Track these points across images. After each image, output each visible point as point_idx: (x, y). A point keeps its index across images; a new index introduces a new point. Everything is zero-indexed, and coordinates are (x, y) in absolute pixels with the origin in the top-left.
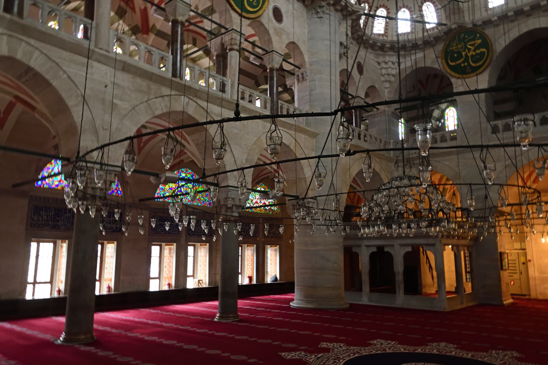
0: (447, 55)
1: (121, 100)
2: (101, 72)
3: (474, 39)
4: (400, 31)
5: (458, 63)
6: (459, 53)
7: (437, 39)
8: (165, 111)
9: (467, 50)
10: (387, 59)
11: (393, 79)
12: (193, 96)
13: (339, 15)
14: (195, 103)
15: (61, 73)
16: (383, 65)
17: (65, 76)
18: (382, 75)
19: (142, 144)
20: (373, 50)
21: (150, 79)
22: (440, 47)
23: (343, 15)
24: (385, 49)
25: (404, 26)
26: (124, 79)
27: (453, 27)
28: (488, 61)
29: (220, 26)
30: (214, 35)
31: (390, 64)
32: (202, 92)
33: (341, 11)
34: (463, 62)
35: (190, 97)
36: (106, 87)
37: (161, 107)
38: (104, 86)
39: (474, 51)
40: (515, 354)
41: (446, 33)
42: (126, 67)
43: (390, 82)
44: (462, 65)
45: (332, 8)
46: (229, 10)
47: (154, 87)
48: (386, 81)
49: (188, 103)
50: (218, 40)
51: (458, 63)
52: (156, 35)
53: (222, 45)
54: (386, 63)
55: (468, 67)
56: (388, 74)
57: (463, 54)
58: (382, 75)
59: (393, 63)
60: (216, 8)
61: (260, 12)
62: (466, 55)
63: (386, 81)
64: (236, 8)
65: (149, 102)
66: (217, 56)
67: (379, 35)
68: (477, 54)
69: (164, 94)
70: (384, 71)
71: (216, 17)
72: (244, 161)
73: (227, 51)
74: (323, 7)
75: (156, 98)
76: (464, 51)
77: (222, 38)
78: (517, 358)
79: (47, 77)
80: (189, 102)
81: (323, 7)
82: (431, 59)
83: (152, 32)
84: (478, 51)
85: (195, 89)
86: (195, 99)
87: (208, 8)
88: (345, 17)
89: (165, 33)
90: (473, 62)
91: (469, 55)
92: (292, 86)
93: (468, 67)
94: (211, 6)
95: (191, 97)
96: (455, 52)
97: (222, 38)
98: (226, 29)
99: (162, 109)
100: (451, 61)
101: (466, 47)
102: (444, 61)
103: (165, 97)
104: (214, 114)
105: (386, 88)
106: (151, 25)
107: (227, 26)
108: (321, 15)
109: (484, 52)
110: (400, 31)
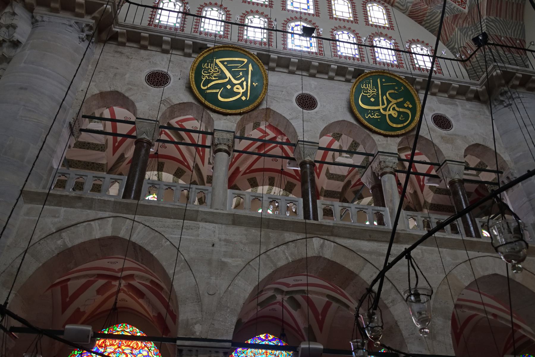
1: (232, 257)
2: (208, 231)
8: (290, 260)
12: (329, 235)
14: (332, 244)
15: (164, 240)
17: (168, 243)
19: (320, 317)
21: (268, 227)
26: (237, 233)
29: (368, 155)
32: (339, 227)
35: (324, 237)
36: (213, 245)
37: (283, 256)
38: (211, 245)
42: (236, 220)
45: (521, 90)
46: (369, 136)
47: (274, 235)
49: (322, 246)
50: (369, 170)
52: (325, 196)
53: (374, 173)
60: (358, 141)
64: (377, 130)
65: (268, 253)
66: (372, 188)
69: (287, 240)
71: (360, 149)
74: (506, 92)
75: (278, 246)
77: (372, 167)
79: (148, 248)
80: (324, 243)
81: (506, 92)
83: (321, 195)
85: (329, 226)
86: (332, 238)
87: (352, 144)
89: (333, 191)
94: (353, 141)
95: (326, 237)
97: (372, 167)
99: (287, 258)
103: (290, 243)
104: (365, 252)
106: (319, 189)
107: (373, 153)
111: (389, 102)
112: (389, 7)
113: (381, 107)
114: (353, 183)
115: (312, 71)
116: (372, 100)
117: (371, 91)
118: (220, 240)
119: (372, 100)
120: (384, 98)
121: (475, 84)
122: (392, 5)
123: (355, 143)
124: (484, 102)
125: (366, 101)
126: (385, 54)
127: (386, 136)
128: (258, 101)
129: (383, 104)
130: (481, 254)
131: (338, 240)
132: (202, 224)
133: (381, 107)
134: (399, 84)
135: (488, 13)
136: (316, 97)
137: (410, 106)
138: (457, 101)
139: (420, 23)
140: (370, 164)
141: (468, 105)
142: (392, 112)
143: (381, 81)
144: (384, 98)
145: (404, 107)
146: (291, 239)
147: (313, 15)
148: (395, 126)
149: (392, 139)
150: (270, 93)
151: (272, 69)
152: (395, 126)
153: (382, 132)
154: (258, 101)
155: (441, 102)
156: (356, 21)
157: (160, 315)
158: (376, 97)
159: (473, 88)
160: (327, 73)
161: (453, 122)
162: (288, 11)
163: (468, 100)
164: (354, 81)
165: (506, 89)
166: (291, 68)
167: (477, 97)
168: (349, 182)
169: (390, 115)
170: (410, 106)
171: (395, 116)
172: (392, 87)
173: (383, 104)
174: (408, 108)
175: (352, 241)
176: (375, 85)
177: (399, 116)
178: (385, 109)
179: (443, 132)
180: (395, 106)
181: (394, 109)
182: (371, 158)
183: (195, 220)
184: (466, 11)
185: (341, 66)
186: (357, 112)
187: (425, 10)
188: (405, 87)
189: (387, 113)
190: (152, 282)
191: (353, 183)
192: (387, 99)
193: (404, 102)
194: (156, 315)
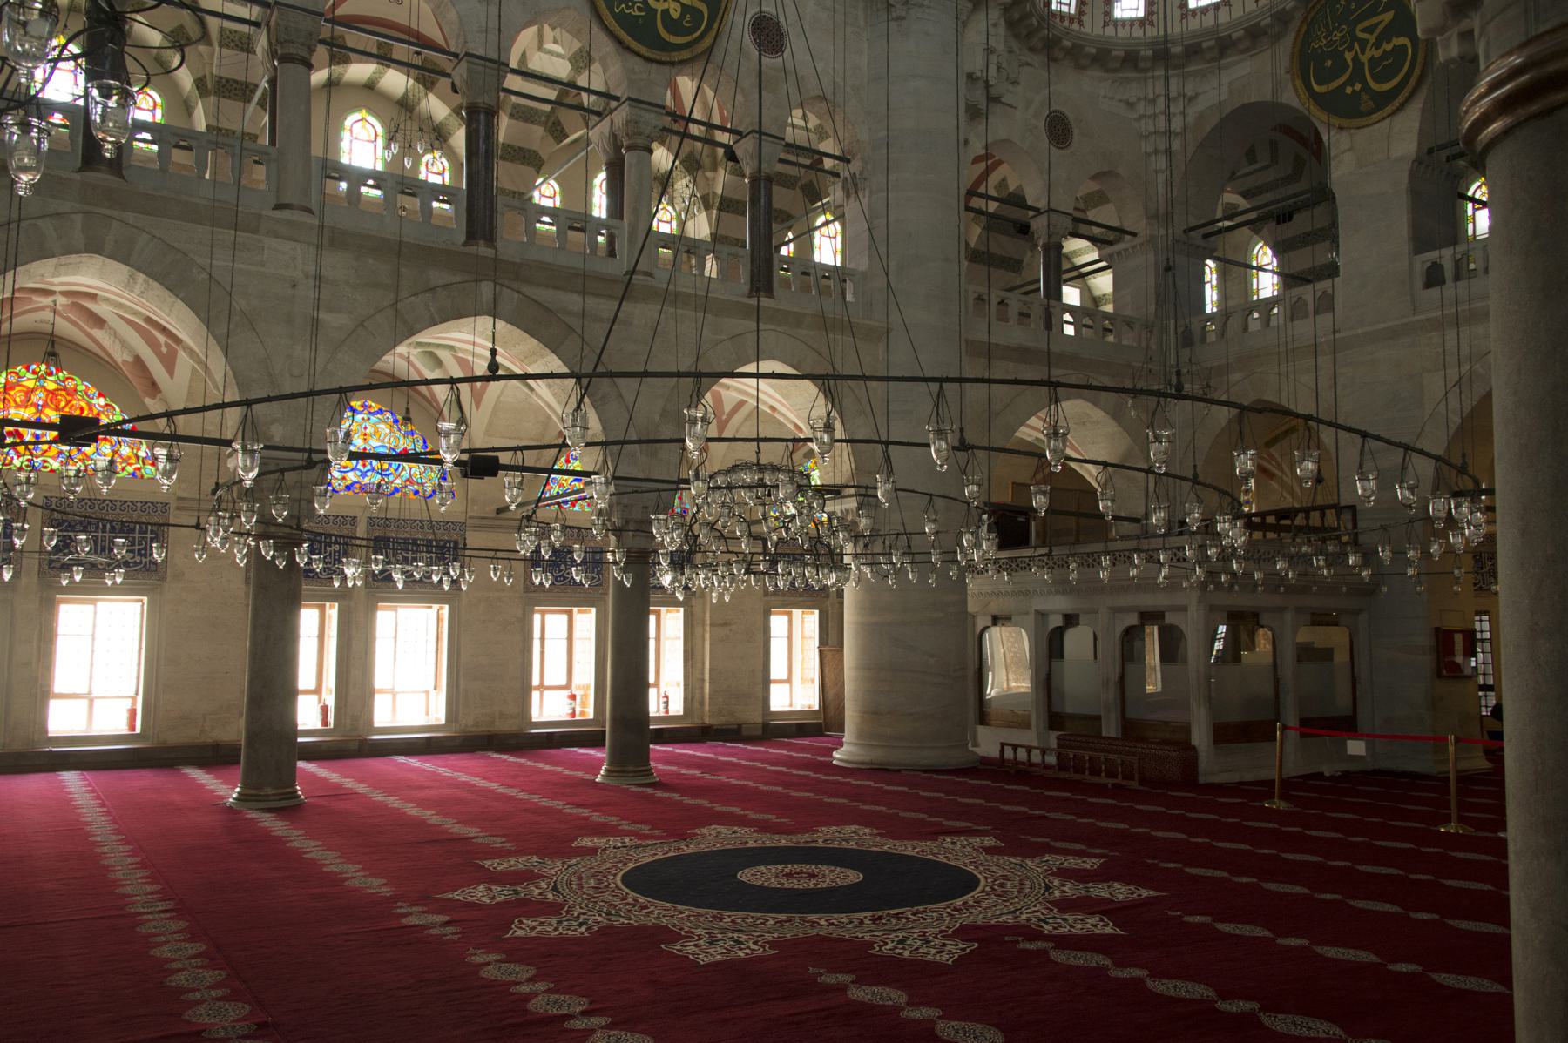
0: (1307, 64)
3: (1373, 12)
5: (1334, 85)
6: (1338, 56)
9: (1356, 46)
14: (516, 295)
20: (1107, 71)
22: (1286, 46)
24: (1142, 65)
28: (1417, 71)
30: (598, 114)
34: (1350, 82)
39: (1377, 45)
40: (989, 841)
44: (1349, 90)
50: (607, 120)
51: (1334, 85)
52: (511, 116)
55: (1365, 96)
57: (1348, 56)
61: (707, 41)
62: (1355, 59)
67: (1132, 22)
68: (1385, 55)
72: (657, 417)
76: (1350, 49)
78: (989, 851)
84: (1389, 47)
90: (1378, 79)
91: (1364, 59)
93: (1365, 96)
98: (617, 99)
100: (1319, 84)
101: (1355, 38)
102: (1299, 82)
105: (1156, 172)
109: (1405, 46)
118: (307, 277)
127: (646, 59)
131: (527, 290)
132: (269, 242)
146: (440, 282)
157: (138, 361)
169: (666, 12)
171: (675, 15)
175: (551, 292)
177: (682, 16)
182: (614, 104)
183: (255, 231)
190: (148, 320)
194: (130, 359)
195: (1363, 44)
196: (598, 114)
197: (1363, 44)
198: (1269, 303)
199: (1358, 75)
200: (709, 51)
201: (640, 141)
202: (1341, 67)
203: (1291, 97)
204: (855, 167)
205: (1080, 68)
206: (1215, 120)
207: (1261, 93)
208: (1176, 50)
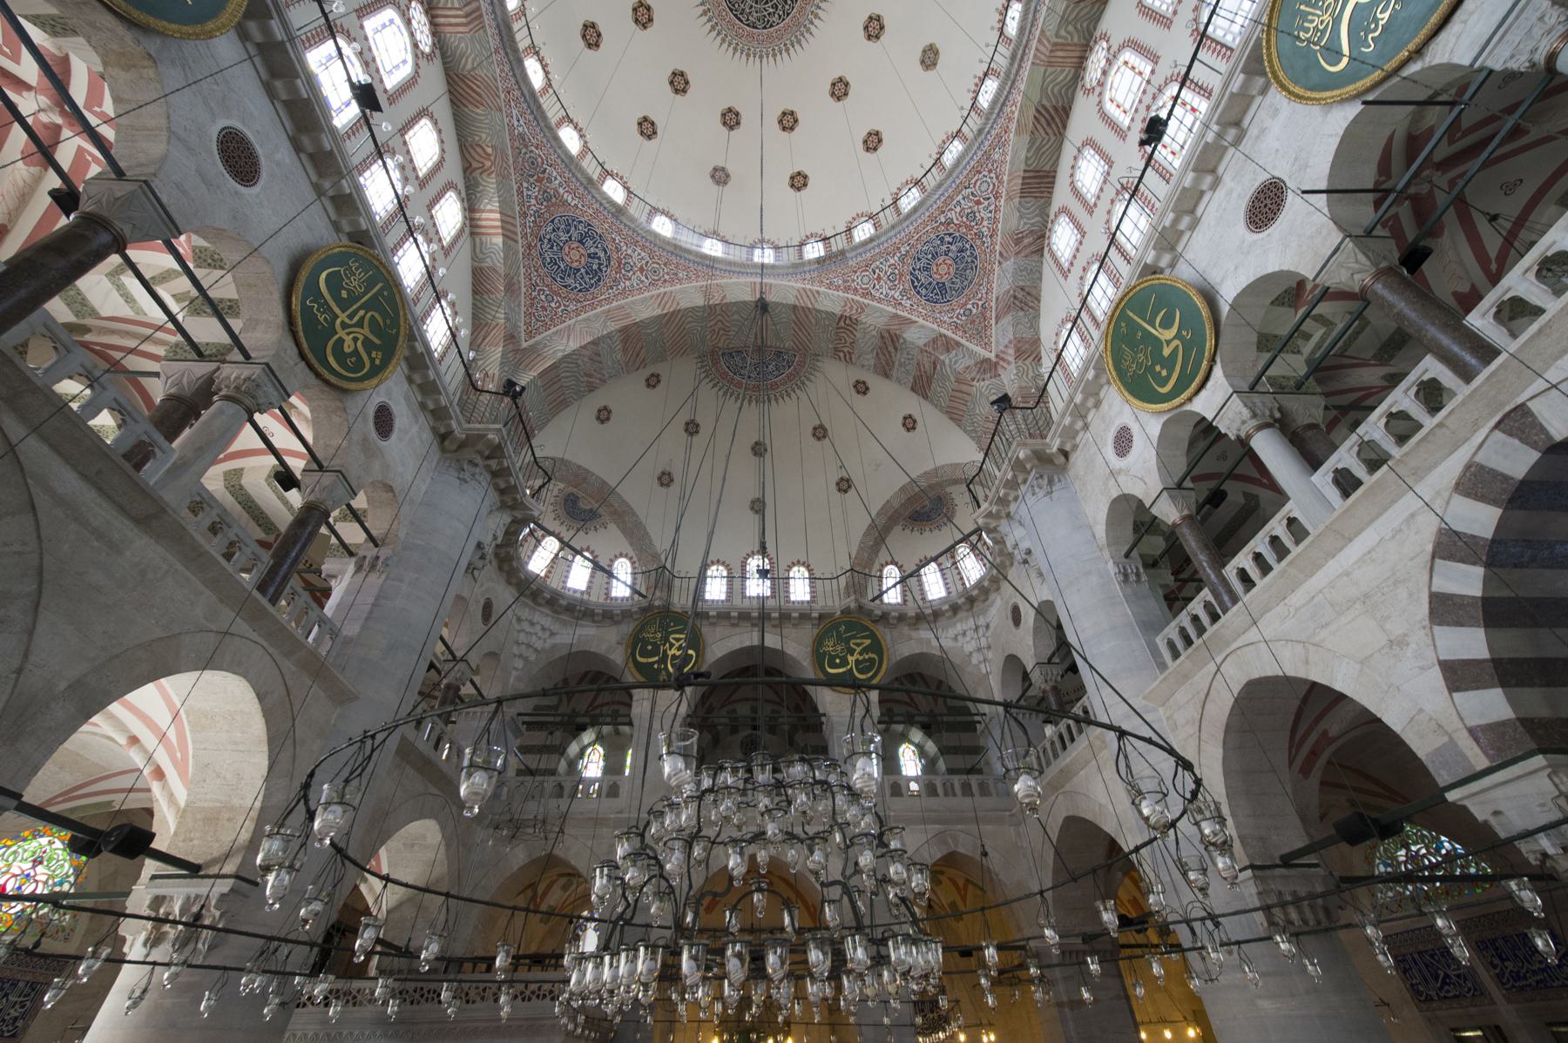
0: (637, 643)
4: (571, 584)
7: (626, 614)
10: (537, 617)
11: (533, 657)
13: (493, 496)
16: (526, 626)
18: (518, 644)
22: (628, 628)
23: (502, 502)
25: (579, 577)
27: (657, 603)
30: (200, 354)
31: (538, 627)
33: (502, 492)
41: (644, 610)
43: (526, 659)
48: (520, 656)
53: (210, 380)
54: (532, 624)
56: (529, 646)
58: (518, 644)
59: (543, 629)
61: (352, 386)
63: (520, 656)
70: (522, 638)
72: (63, 685)
73: (215, 398)
74: (476, 465)
81: (476, 465)
82: (609, 644)
88: (504, 506)
91: (670, 653)
92: (335, 577)
96: (649, 643)
98: (247, 356)
108: (467, 476)
110: (571, 584)
111: (360, 324)
112: (467, 230)
113: (343, 317)
114: (88, 338)
115: (306, 141)
116: (344, 294)
117: (355, 282)
119: (344, 294)
120: (362, 312)
121: (459, 423)
122: (472, 234)
123: (230, 307)
124: (443, 450)
125: (335, 283)
126: (410, 266)
127: (302, 356)
128: (152, 21)
129: (351, 317)
130: (254, 636)
133: (343, 317)
134: (395, 323)
135: (542, 375)
136: (264, 175)
137: (377, 362)
138: (422, 419)
139: (475, 292)
140: (224, 362)
141: (428, 436)
142: (348, 340)
143: (380, 292)
144: (362, 312)
145: (369, 354)
147: (386, 91)
148: (331, 360)
149: (307, 370)
150: (189, 46)
151: (244, 36)
152: (331, 360)
153: (305, 345)
154: (152, 21)
155: (407, 398)
156: (423, 183)
158: (353, 298)
159: (454, 424)
160: (320, 175)
161: (394, 436)
162: (362, 27)
163: (434, 429)
164: (345, 241)
165: (479, 460)
166: (278, 84)
167: (443, 437)
168: (86, 329)
170: (377, 362)
171: (347, 350)
172: (385, 315)
173: (351, 317)
174: (372, 360)
176: (369, 285)
177: (350, 355)
178: (344, 326)
179: (373, 434)
180: (361, 338)
181: (355, 340)
182: (236, 355)
184: (525, 345)
185: (354, 201)
186: (304, 275)
187: (497, 289)
188: (398, 334)
189: (341, 333)
191: (88, 338)
192: (363, 318)
193: (376, 347)
195: (672, 645)
196: (200, 354)
197: (672, 645)
198: (592, 781)
199: (663, 660)
200: (345, 391)
201: (248, 401)
202: (654, 653)
203: (618, 657)
204: (384, 552)
205: (509, 583)
206: (565, 652)
207: (600, 648)
208: (564, 603)
